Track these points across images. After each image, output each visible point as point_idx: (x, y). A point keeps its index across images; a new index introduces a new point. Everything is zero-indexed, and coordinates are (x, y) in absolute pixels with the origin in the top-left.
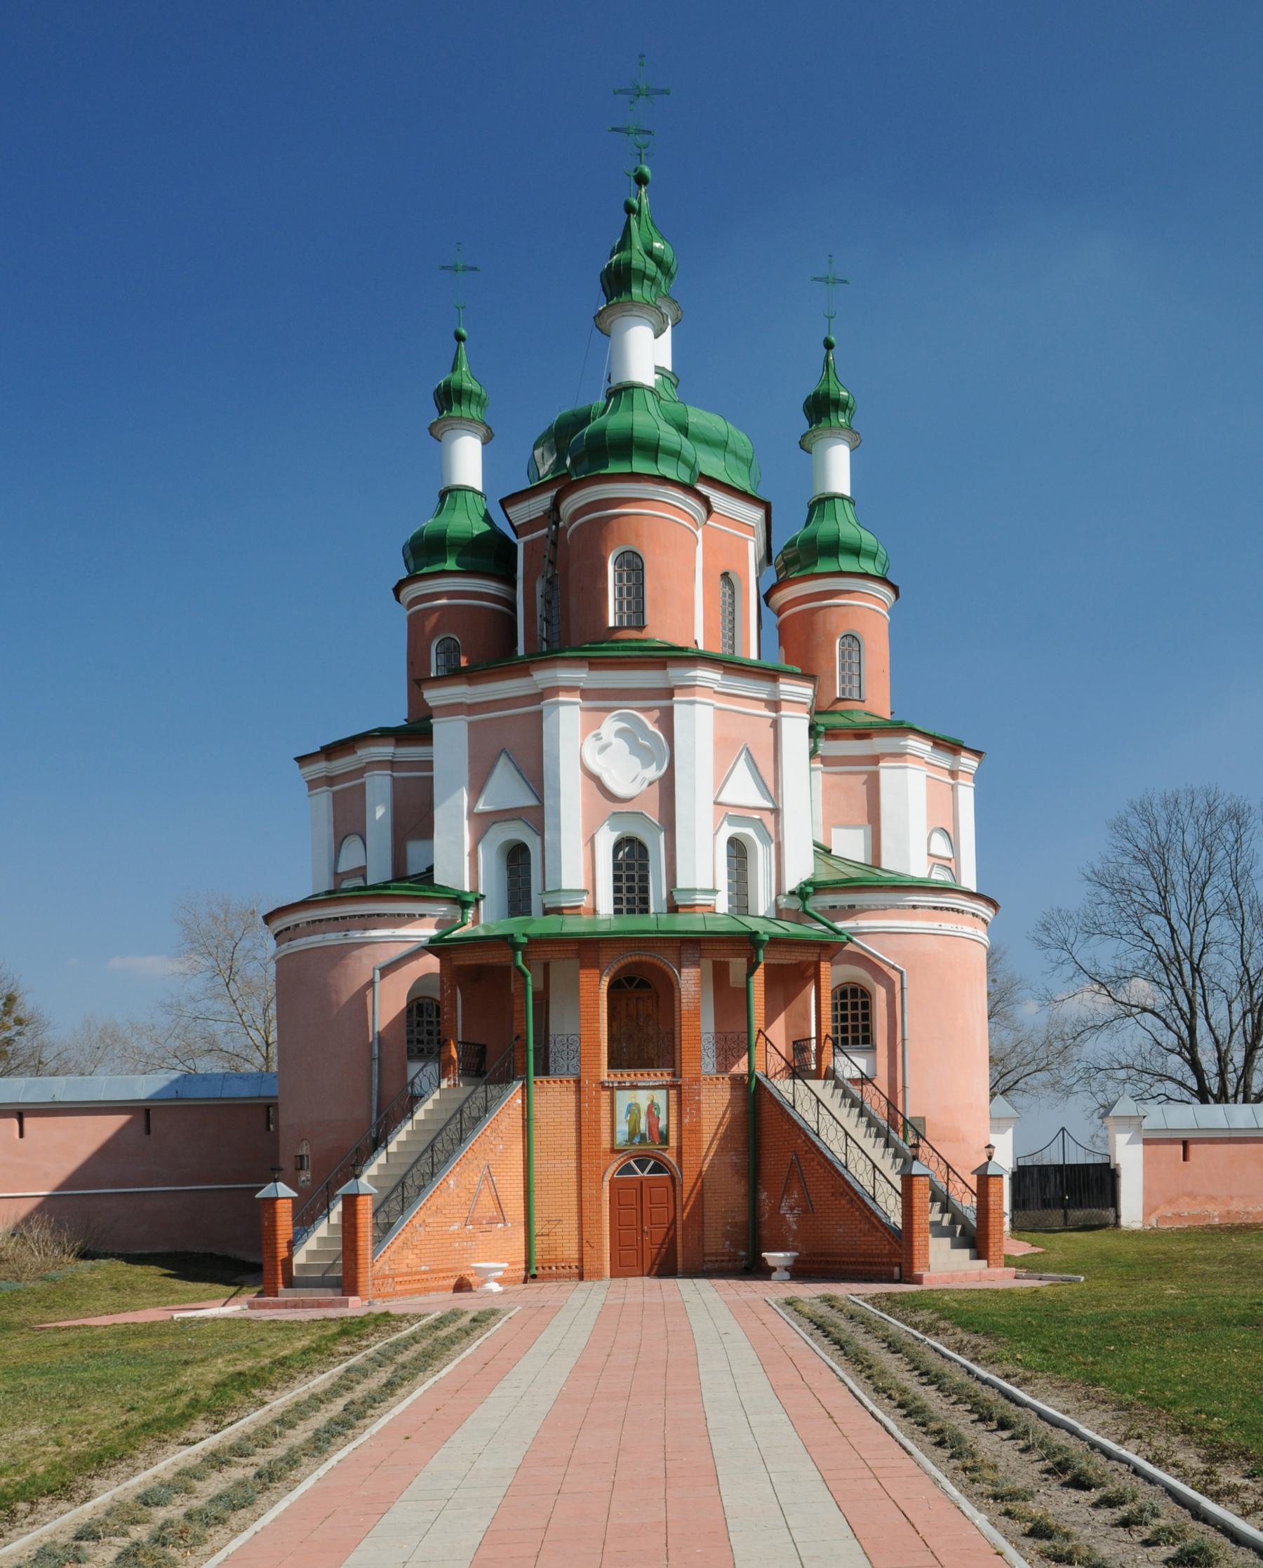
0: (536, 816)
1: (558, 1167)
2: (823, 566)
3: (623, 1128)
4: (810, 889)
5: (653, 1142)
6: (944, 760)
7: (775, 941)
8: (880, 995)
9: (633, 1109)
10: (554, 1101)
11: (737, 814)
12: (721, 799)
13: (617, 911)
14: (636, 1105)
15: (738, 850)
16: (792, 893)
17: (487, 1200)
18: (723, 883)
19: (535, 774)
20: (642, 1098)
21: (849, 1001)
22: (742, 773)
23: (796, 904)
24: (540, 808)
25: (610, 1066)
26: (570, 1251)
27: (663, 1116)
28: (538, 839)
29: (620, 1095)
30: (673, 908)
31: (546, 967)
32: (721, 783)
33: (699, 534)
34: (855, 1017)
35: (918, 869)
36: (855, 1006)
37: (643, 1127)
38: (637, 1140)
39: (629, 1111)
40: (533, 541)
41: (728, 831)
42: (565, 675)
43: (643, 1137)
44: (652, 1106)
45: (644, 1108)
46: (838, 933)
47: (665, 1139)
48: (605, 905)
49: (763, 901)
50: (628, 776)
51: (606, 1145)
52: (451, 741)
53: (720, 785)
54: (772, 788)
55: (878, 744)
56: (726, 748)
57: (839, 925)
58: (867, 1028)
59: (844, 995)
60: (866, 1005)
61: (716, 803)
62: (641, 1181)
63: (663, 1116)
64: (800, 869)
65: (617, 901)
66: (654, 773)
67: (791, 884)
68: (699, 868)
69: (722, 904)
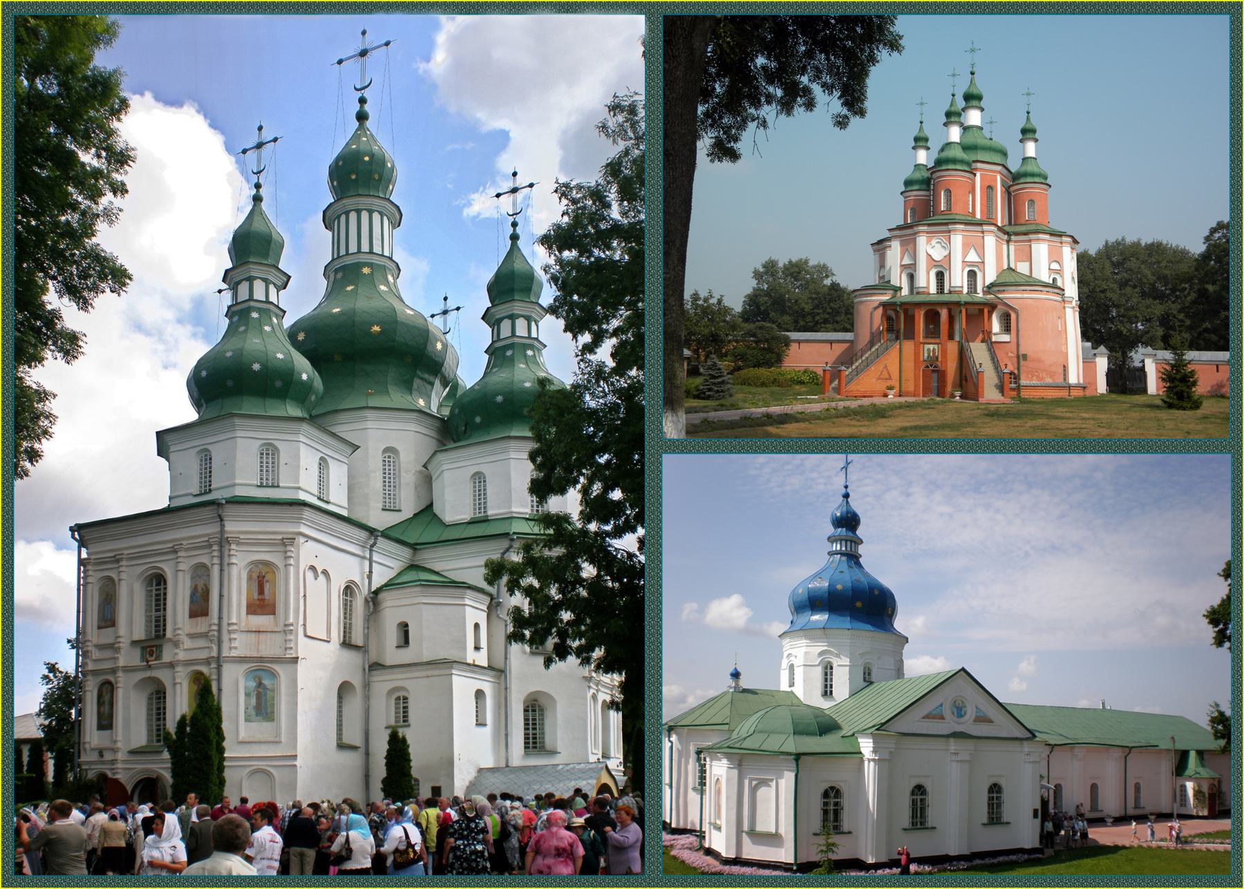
1: (909, 365)
2: (1022, 180)
6: (1058, 239)
7: (966, 303)
8: (1013, 316)
10: (908, 346)
11: (972, 264)
15: (972, 274)
17: (885, 372)
19: (914, 256)
20: (931, 347)
22: (972, 251)
24: (915, 264)
26: (912, 389)
30: (950, 292)
32: (965, 254)
35: (1045, 277)
41: (967, 269)
42: (921, 228)
50: (938, 254)
54: (981, 254)
55: (1032, 236)
56: (966, 248)
64: (991, 277)
66: (946, 253)
68: (958, 279)
69: (965, 290)
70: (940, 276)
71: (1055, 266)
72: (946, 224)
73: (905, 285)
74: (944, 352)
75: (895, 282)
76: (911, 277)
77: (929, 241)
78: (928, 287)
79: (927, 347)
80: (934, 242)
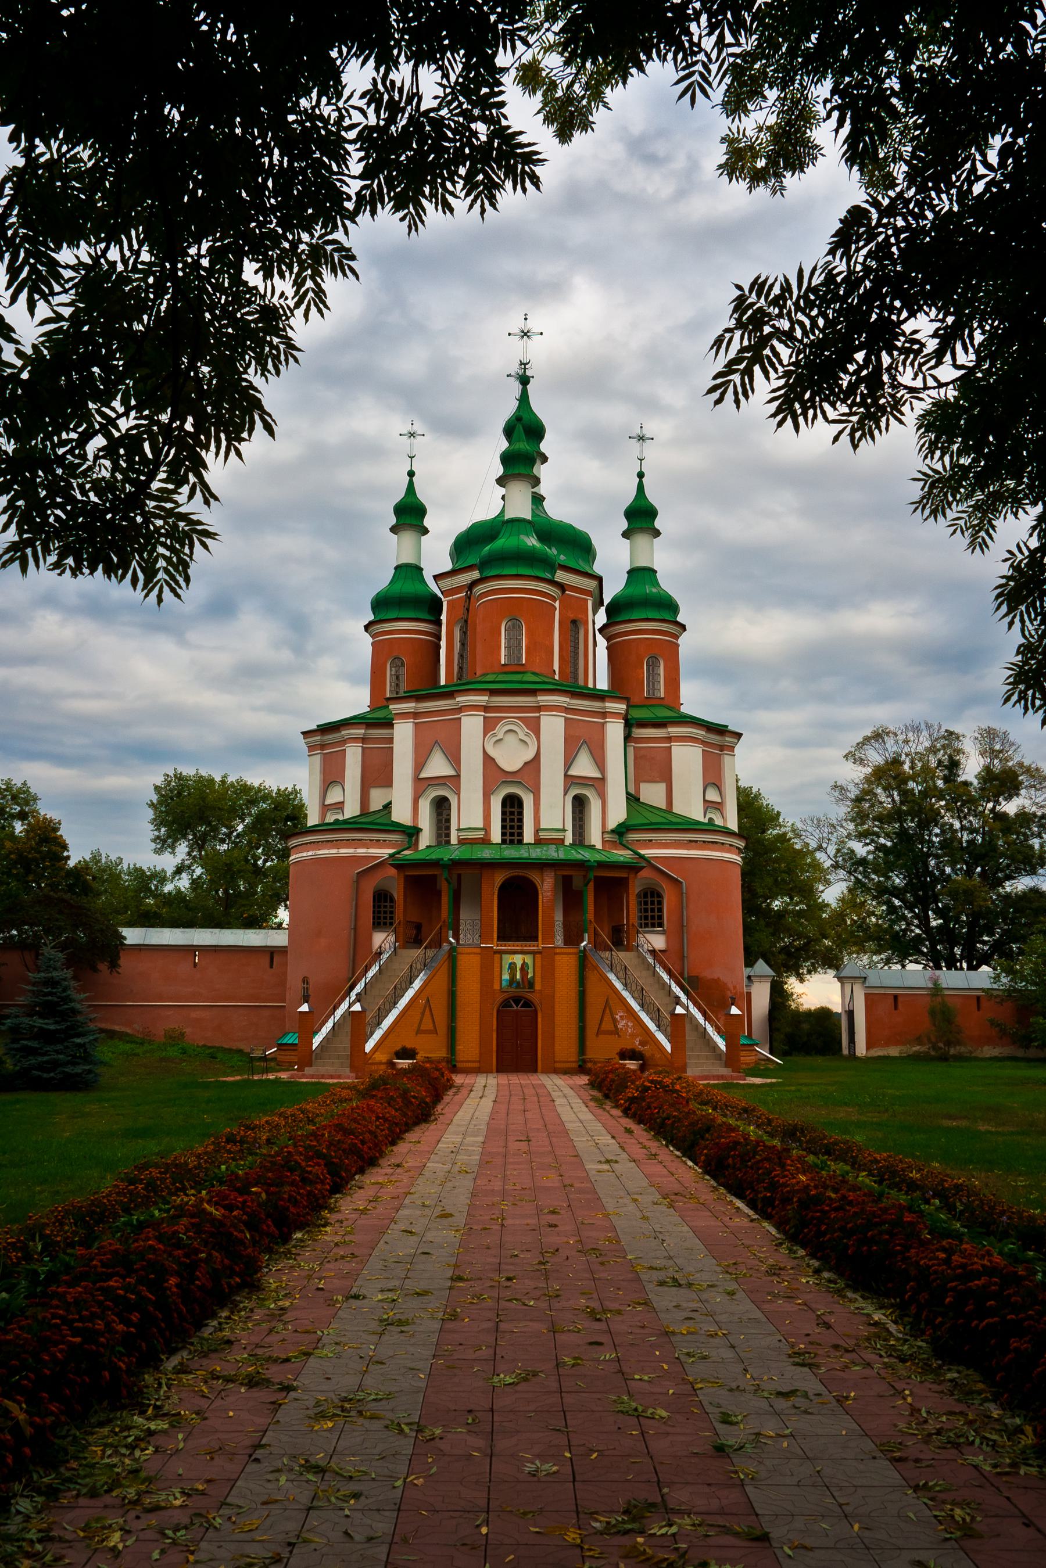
0: (454, 781)
3: (506, 976)
4: (624, 830)
5: (524, 988)
7: (601, 865)
9: (512, 967)
12: (570, 773)
13: (504, 842)
14: (515, 964)
15: (580, 804)
16: (613, 831)
18: (569, 826)
20: (518, 960)
21: (649, 899)
23: (615, 838)
24: (459, 776)
25: (498, 939)
27: (530, 970)
28: (456, 797)
29: (505, 956)
30: (539, 842)
31: (459, 876)
33: (557, 604)
34: (653, 910)
35: (697, 813)
36: (653, 903)
37: (518, 976)
38: (514, 985)
39: (509, 967)
40: (452, 600)
43: (518, 983)
44: (524, 965)
45: (519, 966)
46: (642, 857)
47: (531, 984)
48: (496, 836)
49: (595, 838)
50: (511, 757)
51: (496, 987)
52: (403, 733)
53: (568, 765)
57: (642, 852)
58: (660, 917)
59: (645, 896)
60: (660, 903)
61: (566, 775)
62: (517, 1012)
63: (530, 970)
65: (503, 834)
66: (530, 755)
67: (612, 825)
69: (569, 840)
70: (512, 806)
71: (713, 796)
72: (533, 692)
73: (426, 822)
74: (549, 970)
75: (401, 814)
76: (441, 806)
77: (489, 726)
78: (487, 828)
79: (508, 959)
80: (500, 730)
